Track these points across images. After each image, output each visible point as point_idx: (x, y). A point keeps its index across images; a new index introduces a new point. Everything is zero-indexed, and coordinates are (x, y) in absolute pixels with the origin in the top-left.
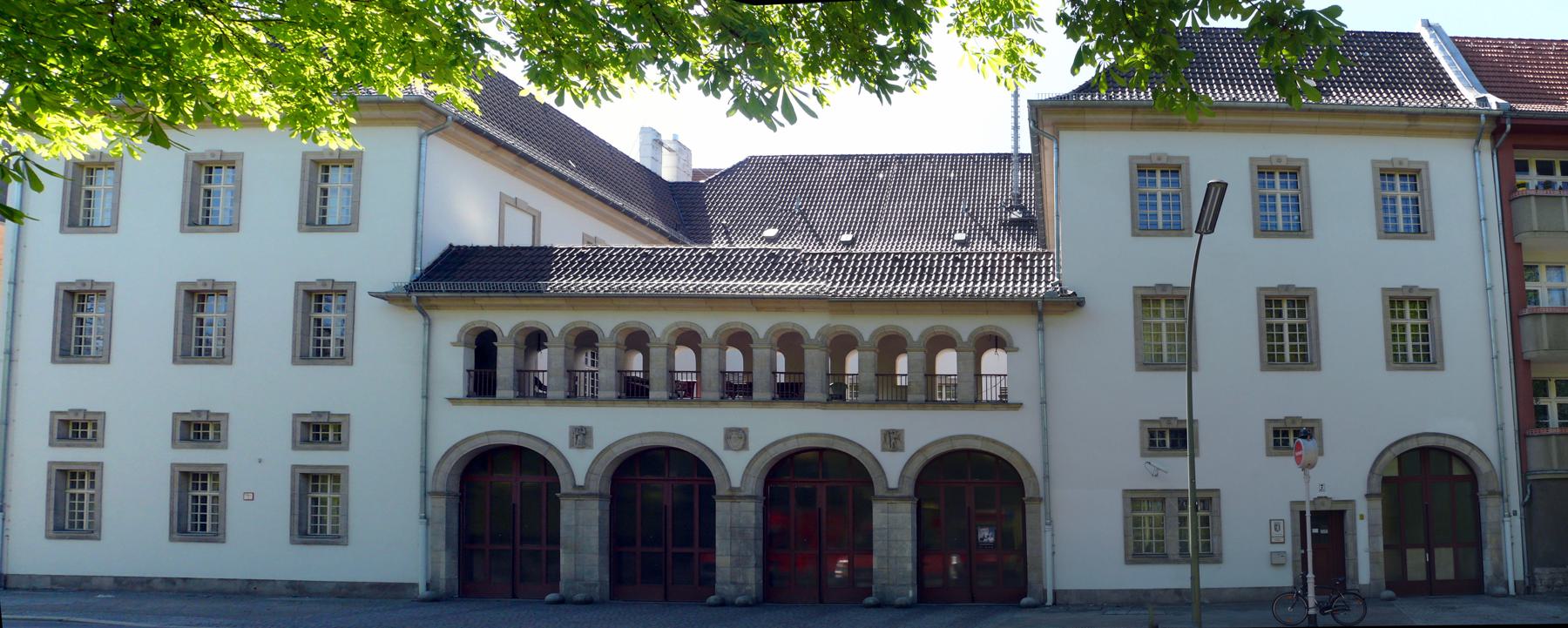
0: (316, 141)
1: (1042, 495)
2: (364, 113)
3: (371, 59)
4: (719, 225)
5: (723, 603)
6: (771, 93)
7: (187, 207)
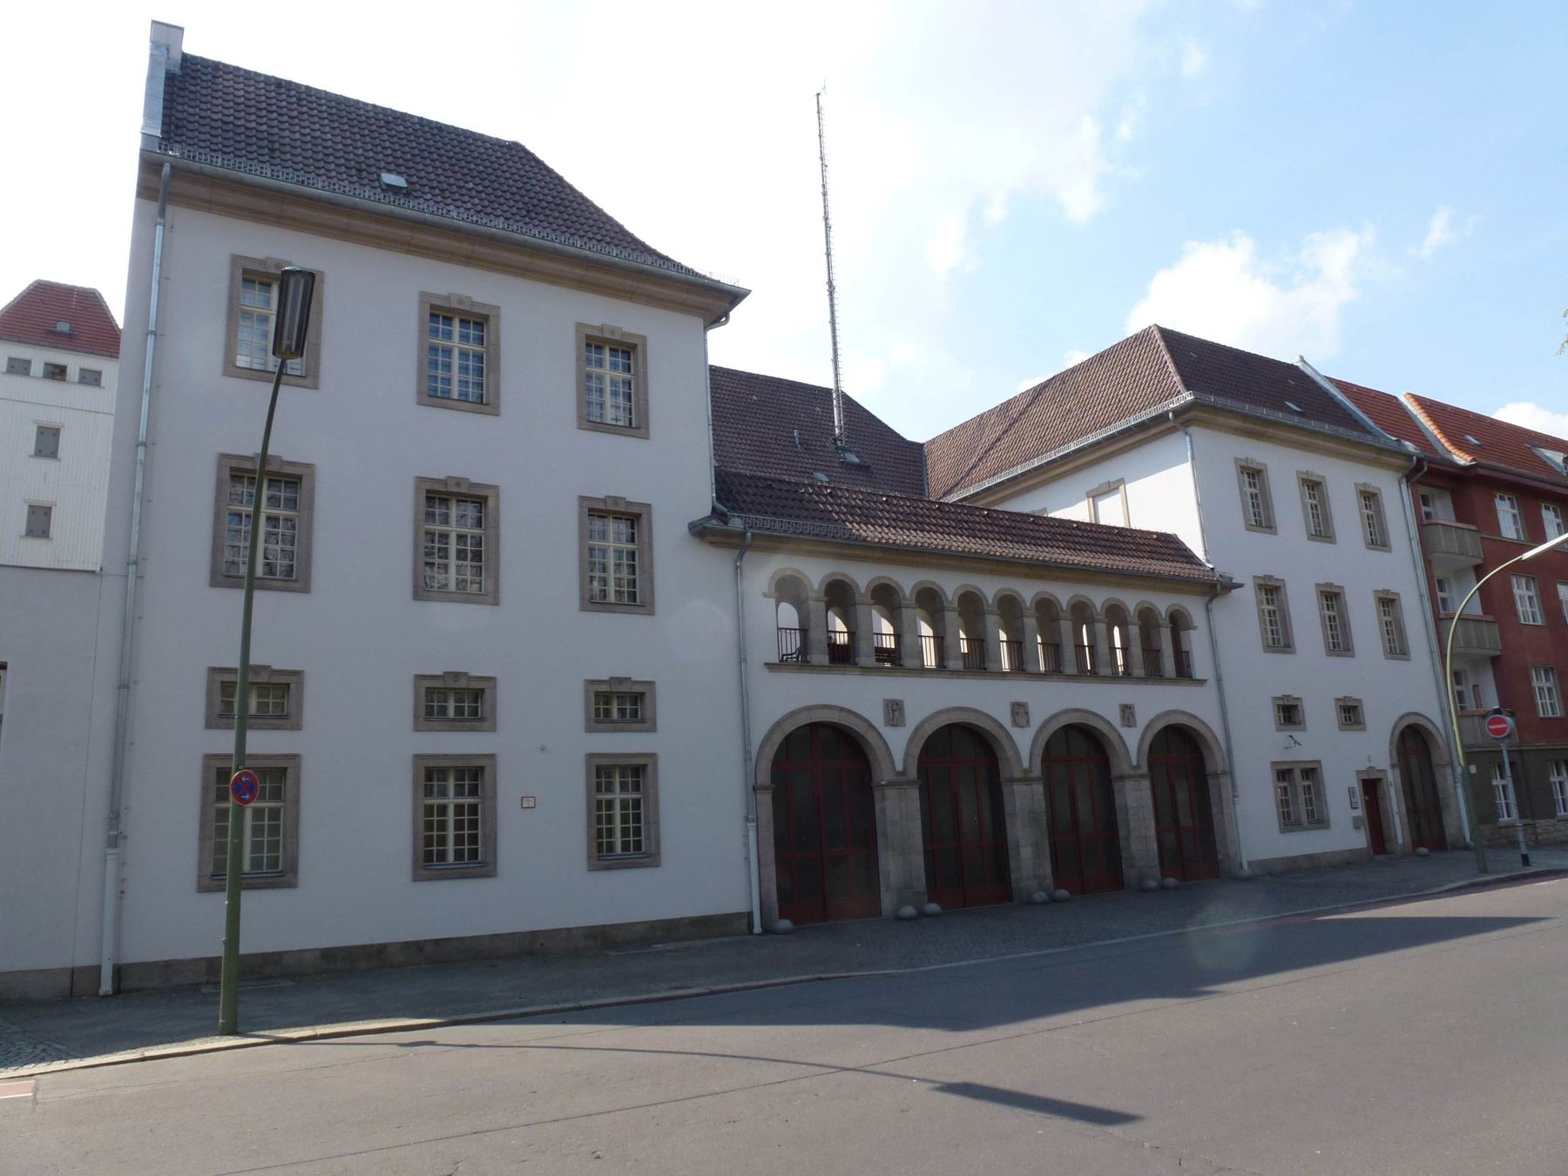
1: (1228, 769)
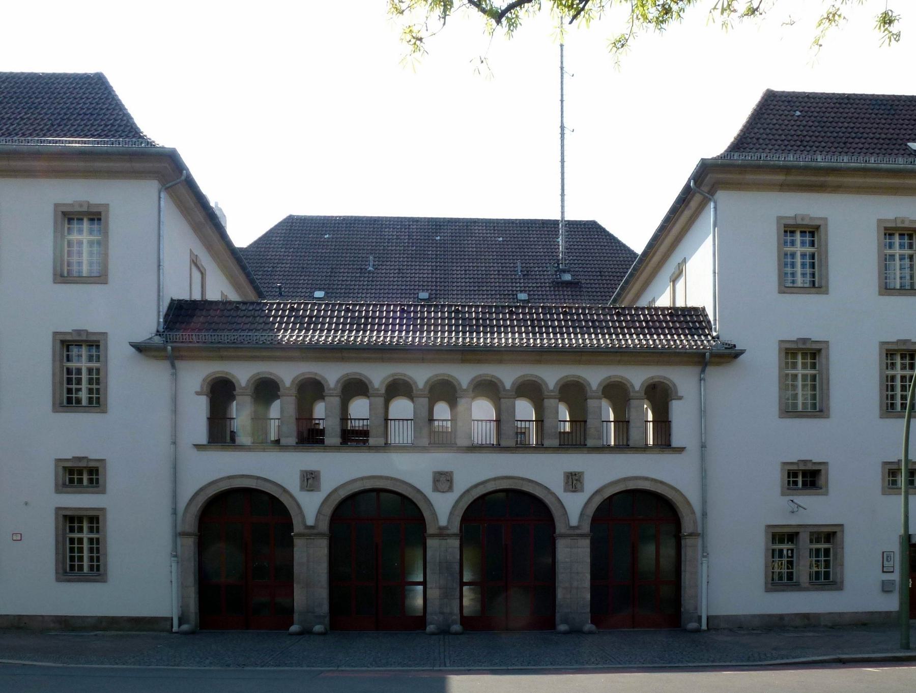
1: (700, 531)
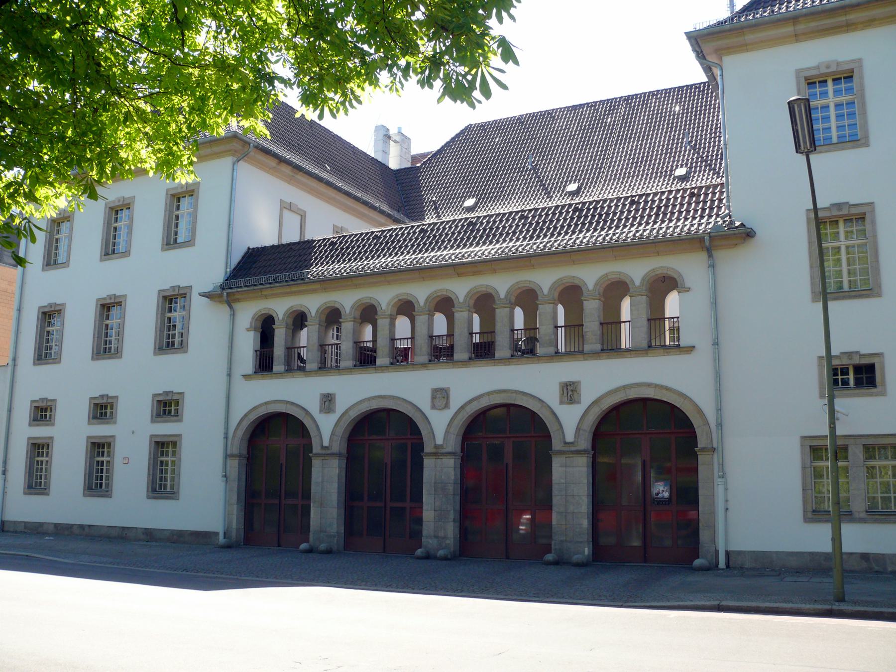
0: (174, 179)
1: (715, 445)
2: (202, 152)
3: (207, 109)
4: (430, 202)
5: (428, 557)
6: (471, 75)
7: (104, 241)
